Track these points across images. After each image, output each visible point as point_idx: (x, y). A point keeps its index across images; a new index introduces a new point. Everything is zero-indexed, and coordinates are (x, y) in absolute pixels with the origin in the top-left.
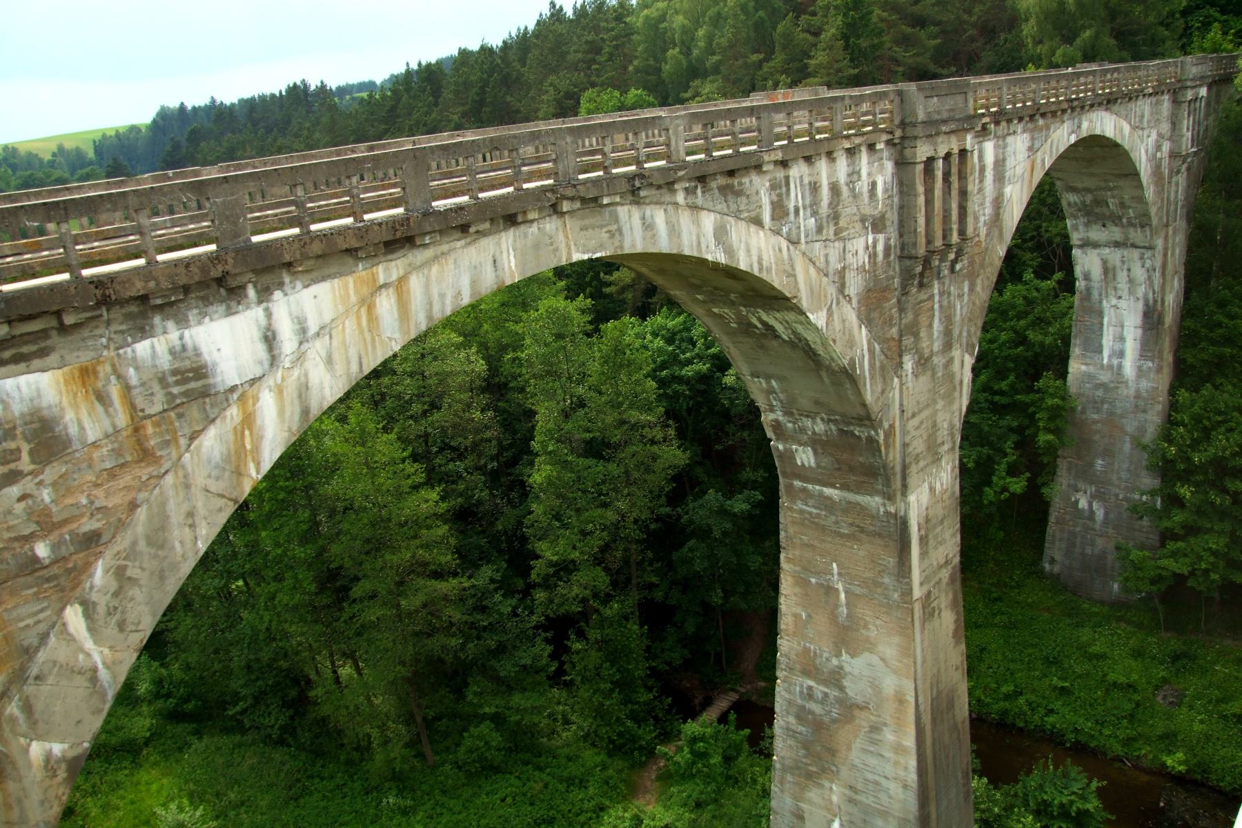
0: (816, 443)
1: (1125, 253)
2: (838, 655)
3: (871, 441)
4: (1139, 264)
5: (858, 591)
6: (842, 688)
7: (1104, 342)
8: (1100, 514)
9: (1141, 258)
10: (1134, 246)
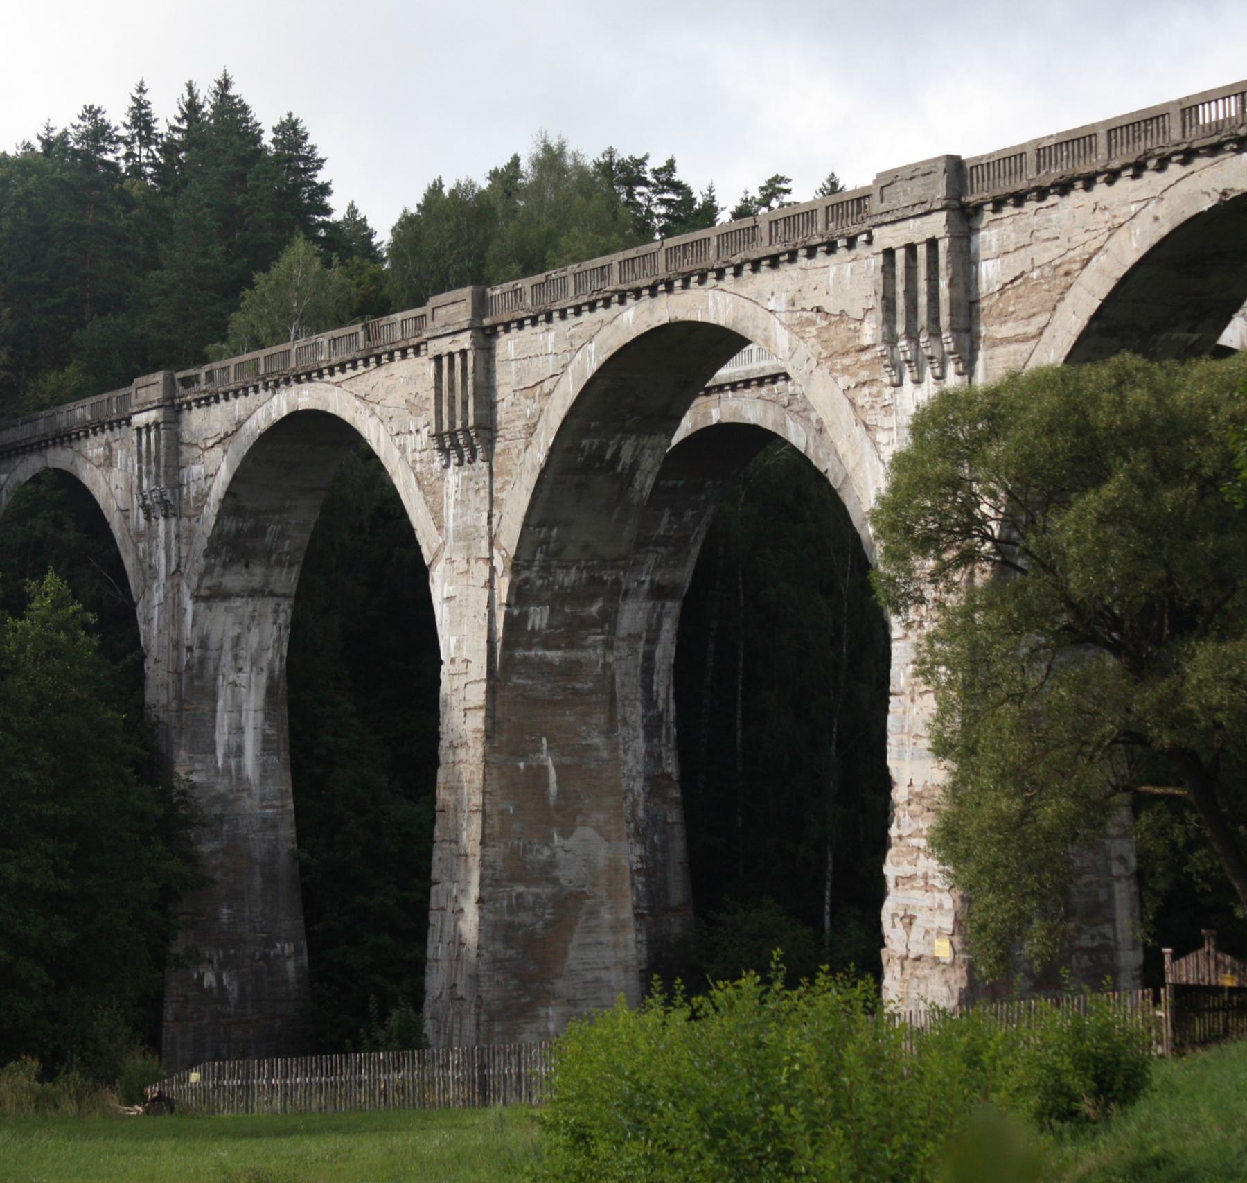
0: (559, 599)
1: (259, 604)
2: (547, 841)
3: (617, 582)
4: (271, 620)
5: (567, 760)
6: (555, 881)
7: (217, 736)
8: (233, 989)
9: (276, 611)
10: (272, 594)
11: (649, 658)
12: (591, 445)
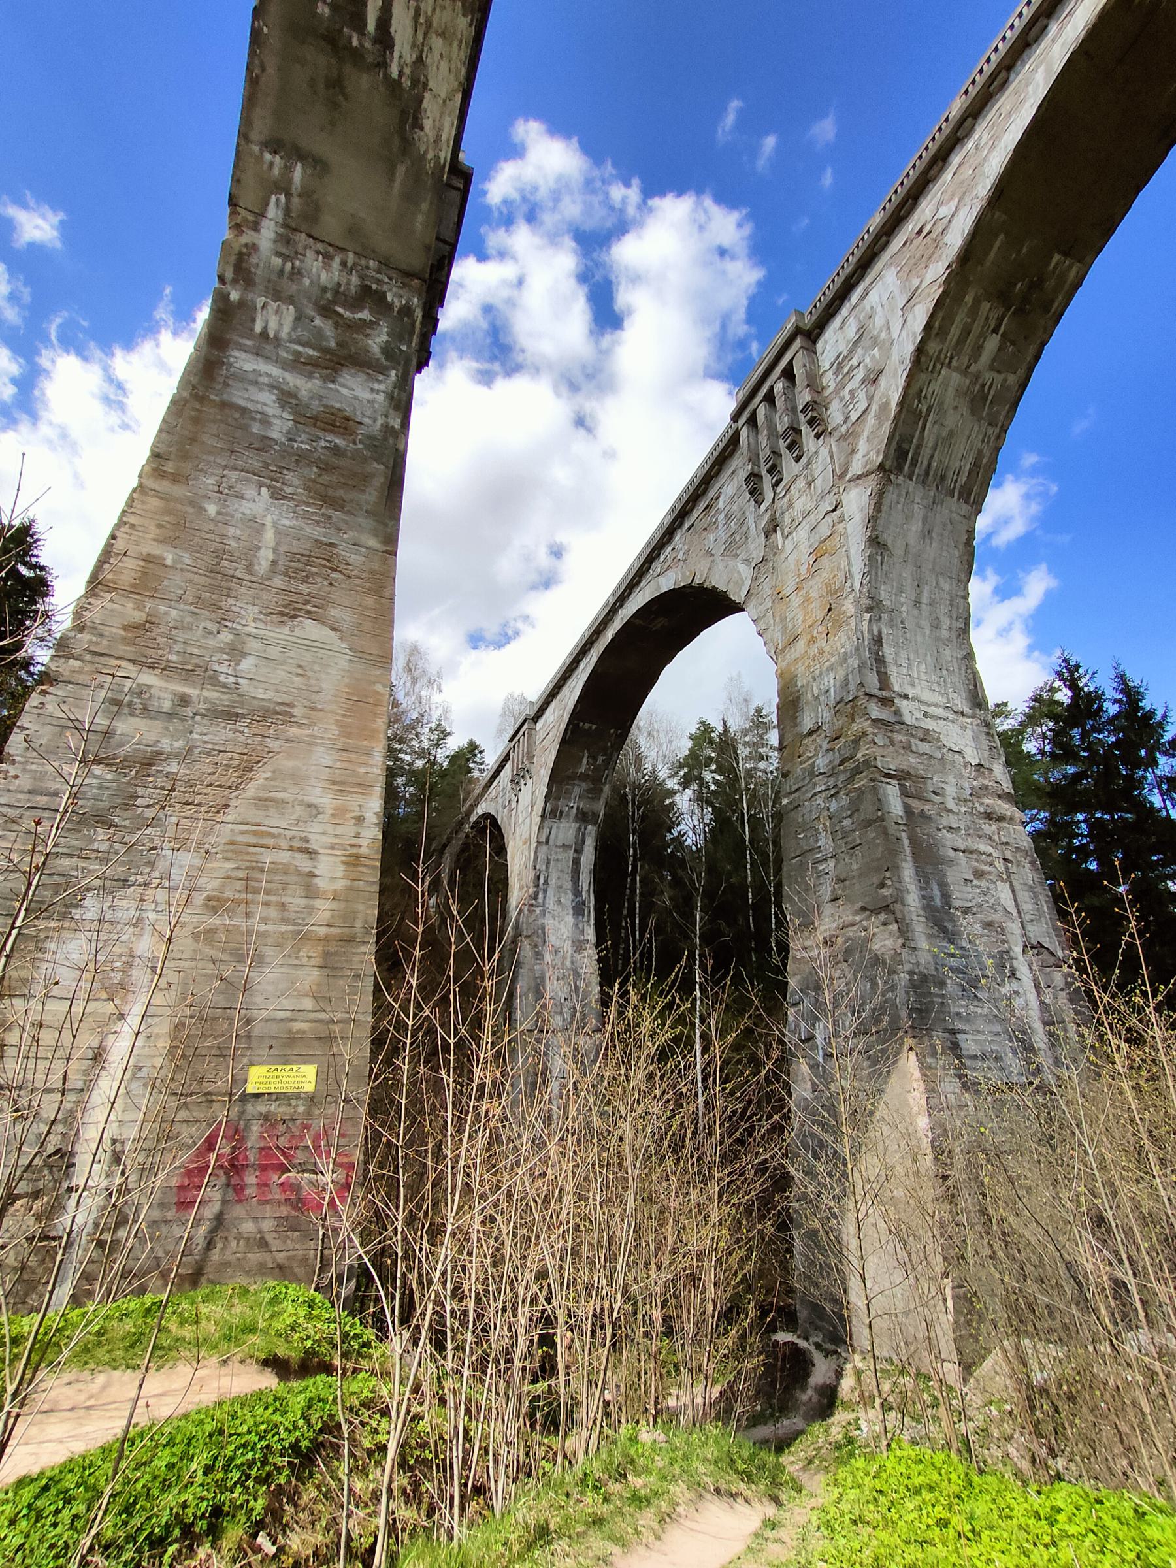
11: (576, 862)
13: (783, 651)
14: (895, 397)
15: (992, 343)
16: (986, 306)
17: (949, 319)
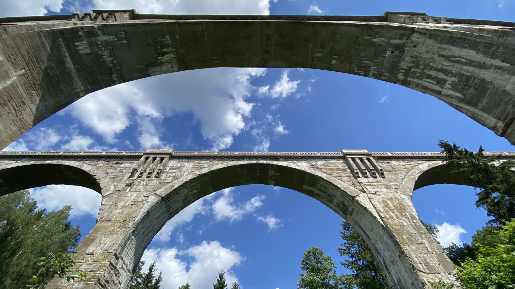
0: (96, 57)
12: (167, 40)
13: (103, 221)
14: (176, 187)
15: (195, 191)
16: (199, 185)
17: (193, 182)
